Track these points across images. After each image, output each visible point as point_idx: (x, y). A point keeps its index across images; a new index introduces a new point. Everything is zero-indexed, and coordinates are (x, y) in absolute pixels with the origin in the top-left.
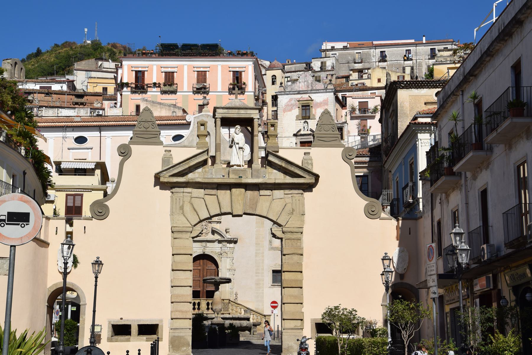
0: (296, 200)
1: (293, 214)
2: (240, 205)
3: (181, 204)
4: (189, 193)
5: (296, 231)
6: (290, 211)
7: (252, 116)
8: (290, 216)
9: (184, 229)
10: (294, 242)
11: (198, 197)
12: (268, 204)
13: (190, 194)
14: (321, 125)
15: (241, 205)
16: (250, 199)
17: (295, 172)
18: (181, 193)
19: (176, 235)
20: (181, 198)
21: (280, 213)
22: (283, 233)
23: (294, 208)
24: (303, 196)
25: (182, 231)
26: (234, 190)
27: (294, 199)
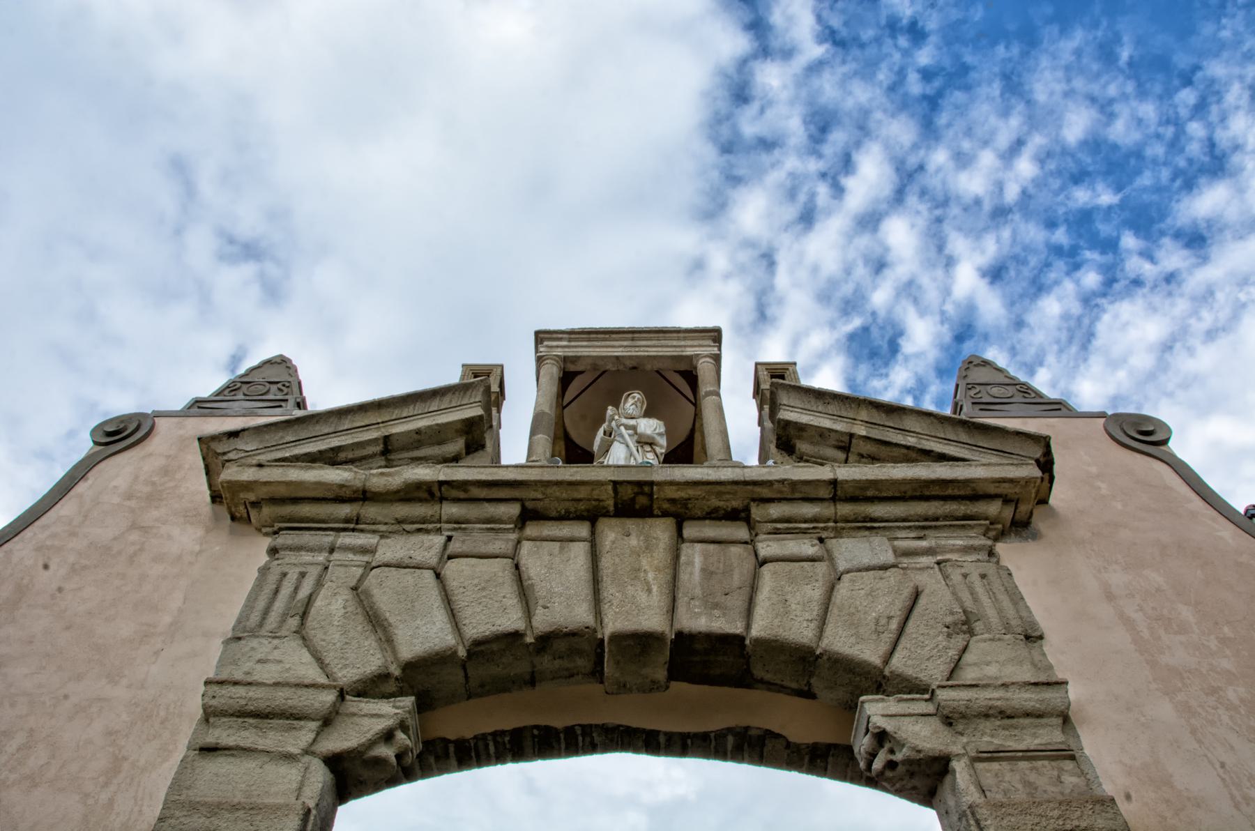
0: (965, 576)
1: (971, 633)
2: (649, 591)
3: (304, 593)
4: (364, 550)
5: (1029, 705)
6: (952, 613)
7: (689, 352)
8: (959, 641)
9: (282, 698)
10: (1032, 769)
11: (407, 561)
12: (815, 592)
13: (366, 558)
14: (976, 386)
15: (655, 588)
16: (703, 570)
17: (928, 448)
18: (320, 549)
19: (223, 734)
20: (313, 572)
21: (894, 625)
22: (948, 721)
23: (969, 604)
24: (998, 562)
25: (262, 705)
26: (611, 533)
27: (956, 576)
